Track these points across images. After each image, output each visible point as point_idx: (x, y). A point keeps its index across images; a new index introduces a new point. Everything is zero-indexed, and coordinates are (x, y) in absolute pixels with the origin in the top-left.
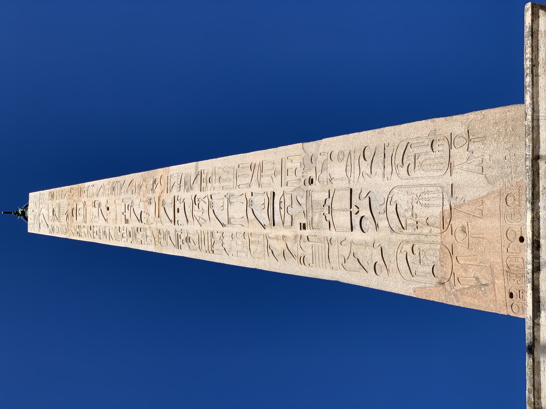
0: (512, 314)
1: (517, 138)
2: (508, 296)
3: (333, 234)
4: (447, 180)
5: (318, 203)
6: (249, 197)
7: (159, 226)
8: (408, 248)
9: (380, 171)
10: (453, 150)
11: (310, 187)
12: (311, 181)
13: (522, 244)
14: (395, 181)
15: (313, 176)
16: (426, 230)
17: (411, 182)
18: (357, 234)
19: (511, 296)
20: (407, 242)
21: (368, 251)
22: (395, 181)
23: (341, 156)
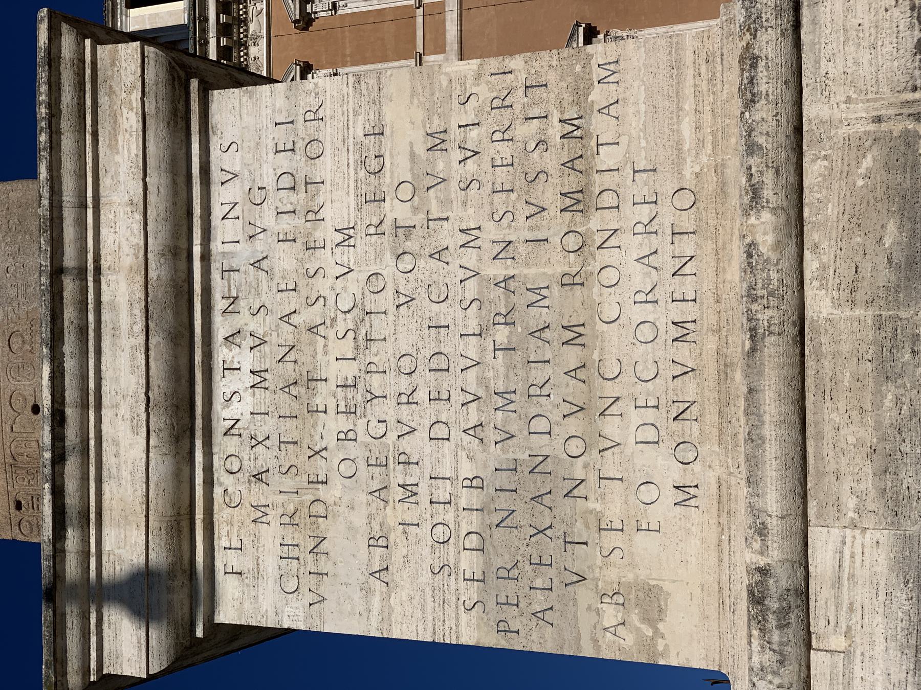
0: (20, 538)
1: (27, 237)
2: (13, 506)
13: (36, 417)
19: (19, 506)
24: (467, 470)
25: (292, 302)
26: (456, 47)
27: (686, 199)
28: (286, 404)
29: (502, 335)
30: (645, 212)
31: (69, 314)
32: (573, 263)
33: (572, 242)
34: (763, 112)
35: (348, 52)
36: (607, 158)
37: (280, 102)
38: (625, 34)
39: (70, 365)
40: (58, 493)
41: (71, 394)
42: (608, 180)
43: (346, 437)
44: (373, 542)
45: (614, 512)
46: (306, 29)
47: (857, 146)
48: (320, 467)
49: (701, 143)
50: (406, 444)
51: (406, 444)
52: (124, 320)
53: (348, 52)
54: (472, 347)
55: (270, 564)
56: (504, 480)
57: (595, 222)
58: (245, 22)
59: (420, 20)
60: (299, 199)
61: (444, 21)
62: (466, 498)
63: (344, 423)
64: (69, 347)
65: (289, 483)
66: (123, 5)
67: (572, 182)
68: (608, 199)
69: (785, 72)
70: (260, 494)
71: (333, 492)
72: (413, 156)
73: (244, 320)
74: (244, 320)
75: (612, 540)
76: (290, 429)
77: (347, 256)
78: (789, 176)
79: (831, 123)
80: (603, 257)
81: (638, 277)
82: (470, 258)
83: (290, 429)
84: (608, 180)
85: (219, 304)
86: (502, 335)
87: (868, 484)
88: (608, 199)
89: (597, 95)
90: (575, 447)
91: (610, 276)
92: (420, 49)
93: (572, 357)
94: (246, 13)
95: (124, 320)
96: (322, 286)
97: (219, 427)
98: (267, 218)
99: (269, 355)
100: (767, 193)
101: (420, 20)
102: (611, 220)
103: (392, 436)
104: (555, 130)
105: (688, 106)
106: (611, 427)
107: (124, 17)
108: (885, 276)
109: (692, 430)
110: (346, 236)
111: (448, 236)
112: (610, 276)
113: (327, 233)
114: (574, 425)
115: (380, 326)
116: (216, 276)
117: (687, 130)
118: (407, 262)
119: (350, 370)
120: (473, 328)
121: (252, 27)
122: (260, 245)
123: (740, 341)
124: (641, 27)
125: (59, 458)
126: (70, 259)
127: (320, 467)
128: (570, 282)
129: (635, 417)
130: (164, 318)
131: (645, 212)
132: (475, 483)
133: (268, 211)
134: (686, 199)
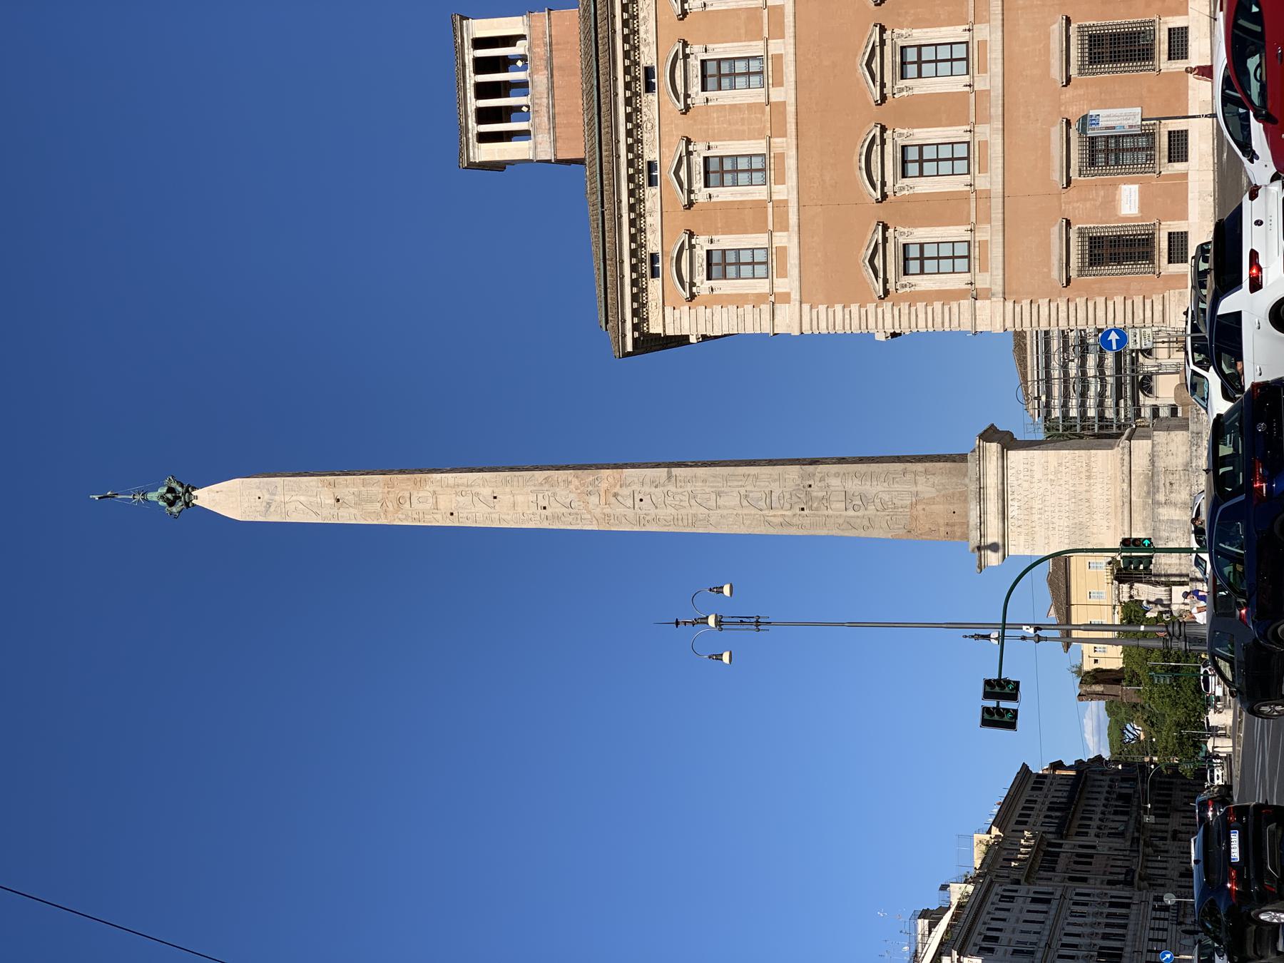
3: (830, 512)
4: (914, 489)
5: (817, 498)
6: (743, 492)
7: (607, 511)
8: (889, 518)
9: (869, 483)
10: (917, 477)
11: (809, 489)
12: (810, 486)
14: (880, 488)
15: (811, 482)
16: (902, 510)
17: (891, 489)
18: (851, 513)
20: (888, 515)
21: (859, 520)
22: (880, 488)
23: (837, 475)
24: (1066, 524)
25: (1027, 493)
26: (796, 229)
27: (1109, 478)
28: (1026, 512)
29: (1073, 500)
30: (1102, 480)
31: (982, 496)
32: (1088, 488)
33: (1087, 484)
34: (1124, 468)
35: (719, 225)
36: (1094, 470)
37: (1025, 454)
38: (906, 230)
39: (982, 506)
40: (980, 531)
41: (982, 512)
42: (1094, 474)
43: (1039, 519)
44: (1045, 538)
45: (1095, 531)
46: (689, 209)
47: (1140, 474)
48: (1034, 524)
49: (1112, 469)
50: (1053, 520)
51: (1053, 520)
52: (992, 497)
53: (719, 225)
54: (1067, 502)
55: (1022, 543)
56: (1074, 526)
57: (1092, 481)
58: (643, 201)
59: (770, 210)
60: (1029, 473)
61: (788, 211)
62: (1066, 529)
63: (1039, 516)
64: (982, 502)
65: (1027, 527)
66: (475, 140)
67: (1088, 474)
68: (1094, 477)
69: (1129, 461)
70: (1019, 530)
71: (1037, 529)
72: (1055, 467)
73: (1015, 496)
74: (1015, 496)
75: (1094, 536)
76: (1027, 517)
77: (1040, 485)
78: (1129, 478)
79: (1135, 471)
80: (1093, 487)
81: (1100, 491)
82: (1067, 486)
83: (1027, 517)
84: (1094, 474)
85: (1009, 493)
86: (1073, 500)
87: (1141, 526)
88: (1094, 477)
89: (1093, 459)
90: (1088, 520)
91: (1095, 491)
92: (771, 228)
93: (1087, 504)
94: (644, 195)
95: (992, 497)
96: (1034, 490)
97: (1010, 517)
98: (1021, 476)
99: (1022, 503)
100: (1126, 480)
101: (770, 210)
102: (1095, 481)
103: (1050, 519)
104: (1084, 465)
105: (1109, 462)
106: (1095, 517)
107: (476, 150)
108: (1144, 494)
109: (1109, 517)
110: (1040, 481)
111: (1062, 482)
112: (1095, 491)
113: (1035, 480)
114: (1087, 516)
115: (1047, 498)
116: (1009, 488)
117: (1109, 466)
118: (1053, 486)
119: (1040, 506)
120: (1067, 498)
121: (648, 204)
122: (1019, 482)
123: (1120, 503)
124: (916, 227)
125: (980, 525)
126: (982, 486)
127: (1034, 524)
128: (1087, 491)
129: (1099, 515)
130: (1000, 496)
131: (1102, 480)
132: (1068, 526)
133: (1021, 476)
134: (1109, 478)
